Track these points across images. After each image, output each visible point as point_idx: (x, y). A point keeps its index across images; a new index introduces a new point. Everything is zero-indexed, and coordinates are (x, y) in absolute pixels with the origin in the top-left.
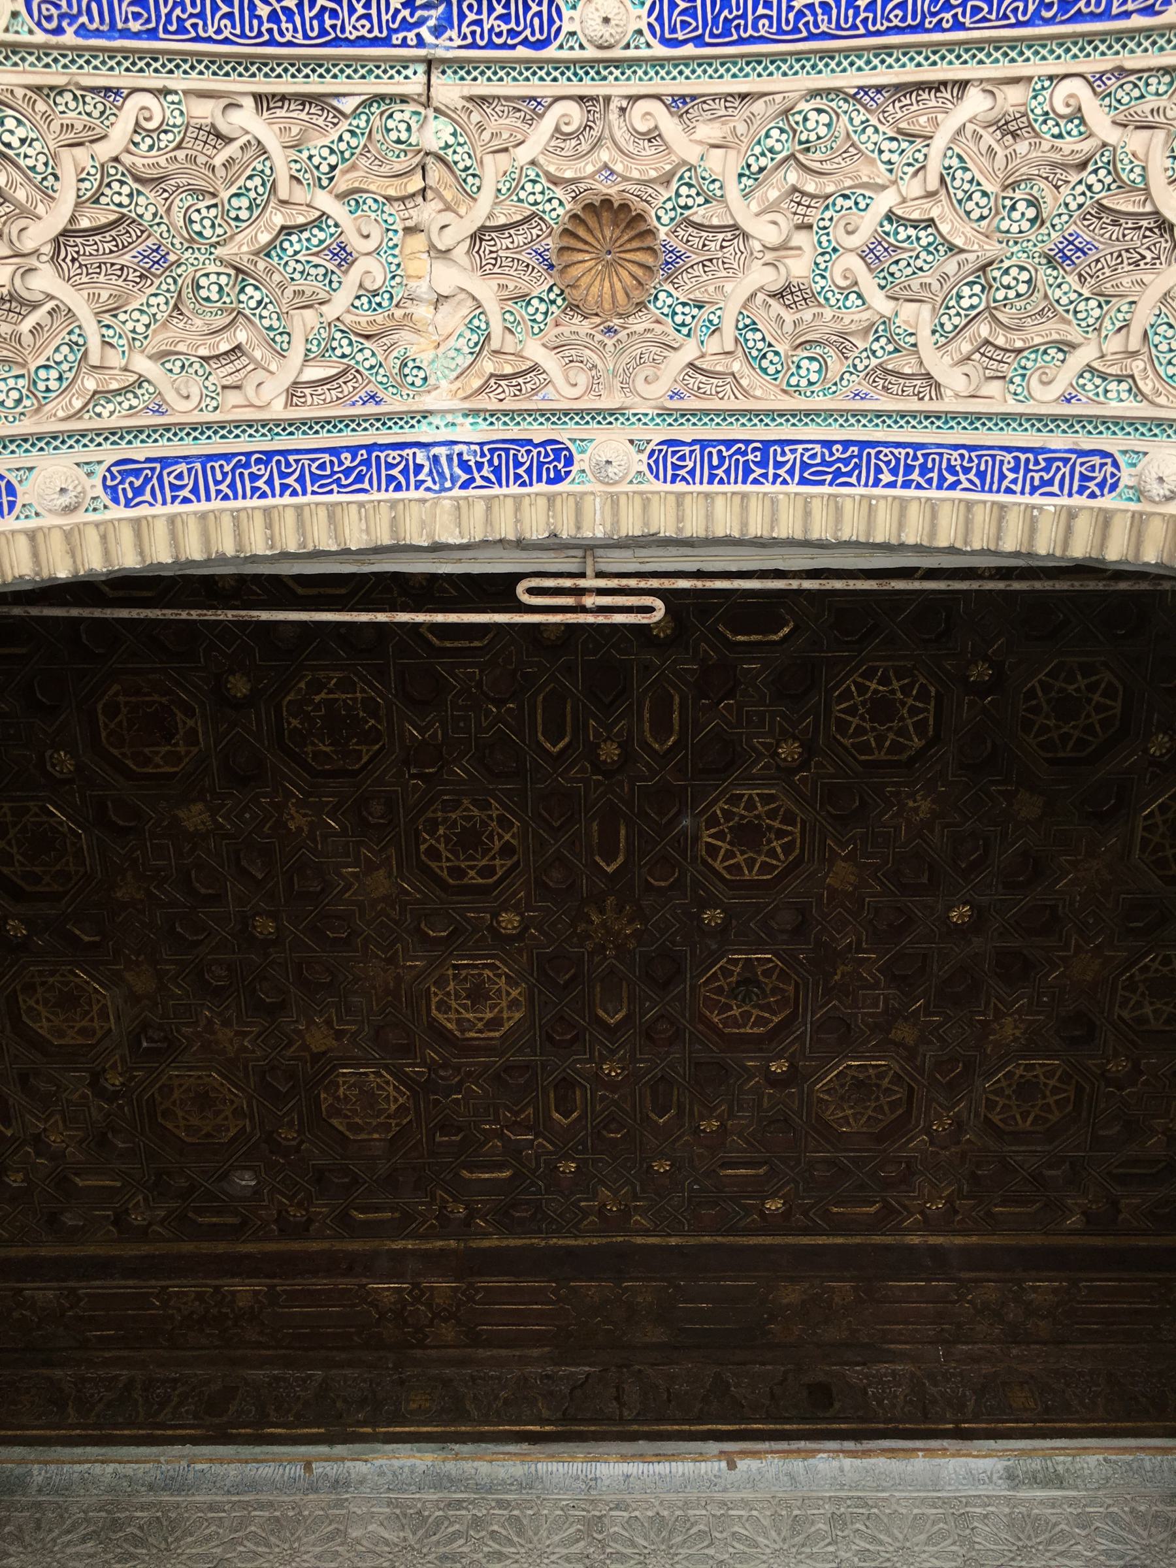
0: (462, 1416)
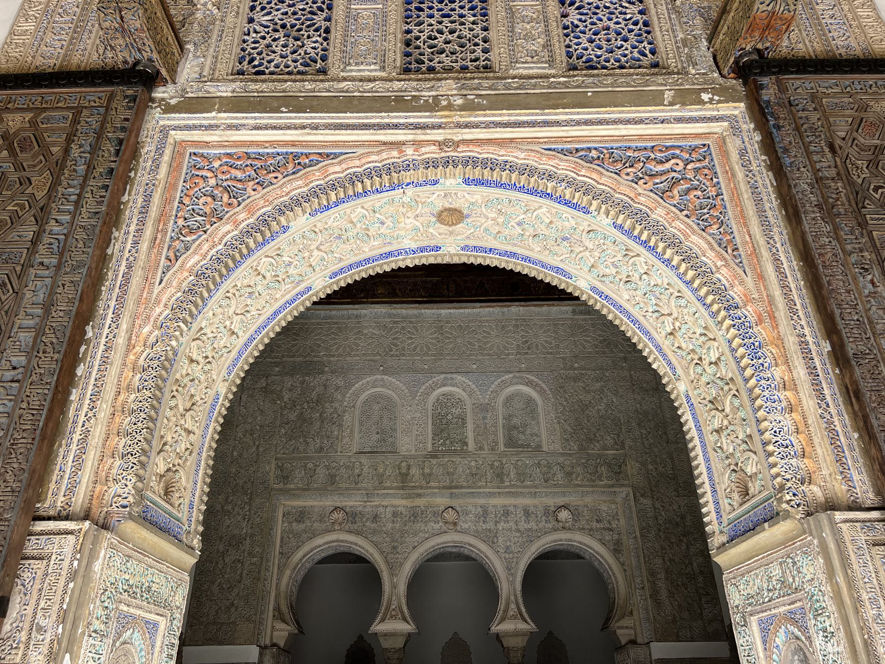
0: (396, 296)
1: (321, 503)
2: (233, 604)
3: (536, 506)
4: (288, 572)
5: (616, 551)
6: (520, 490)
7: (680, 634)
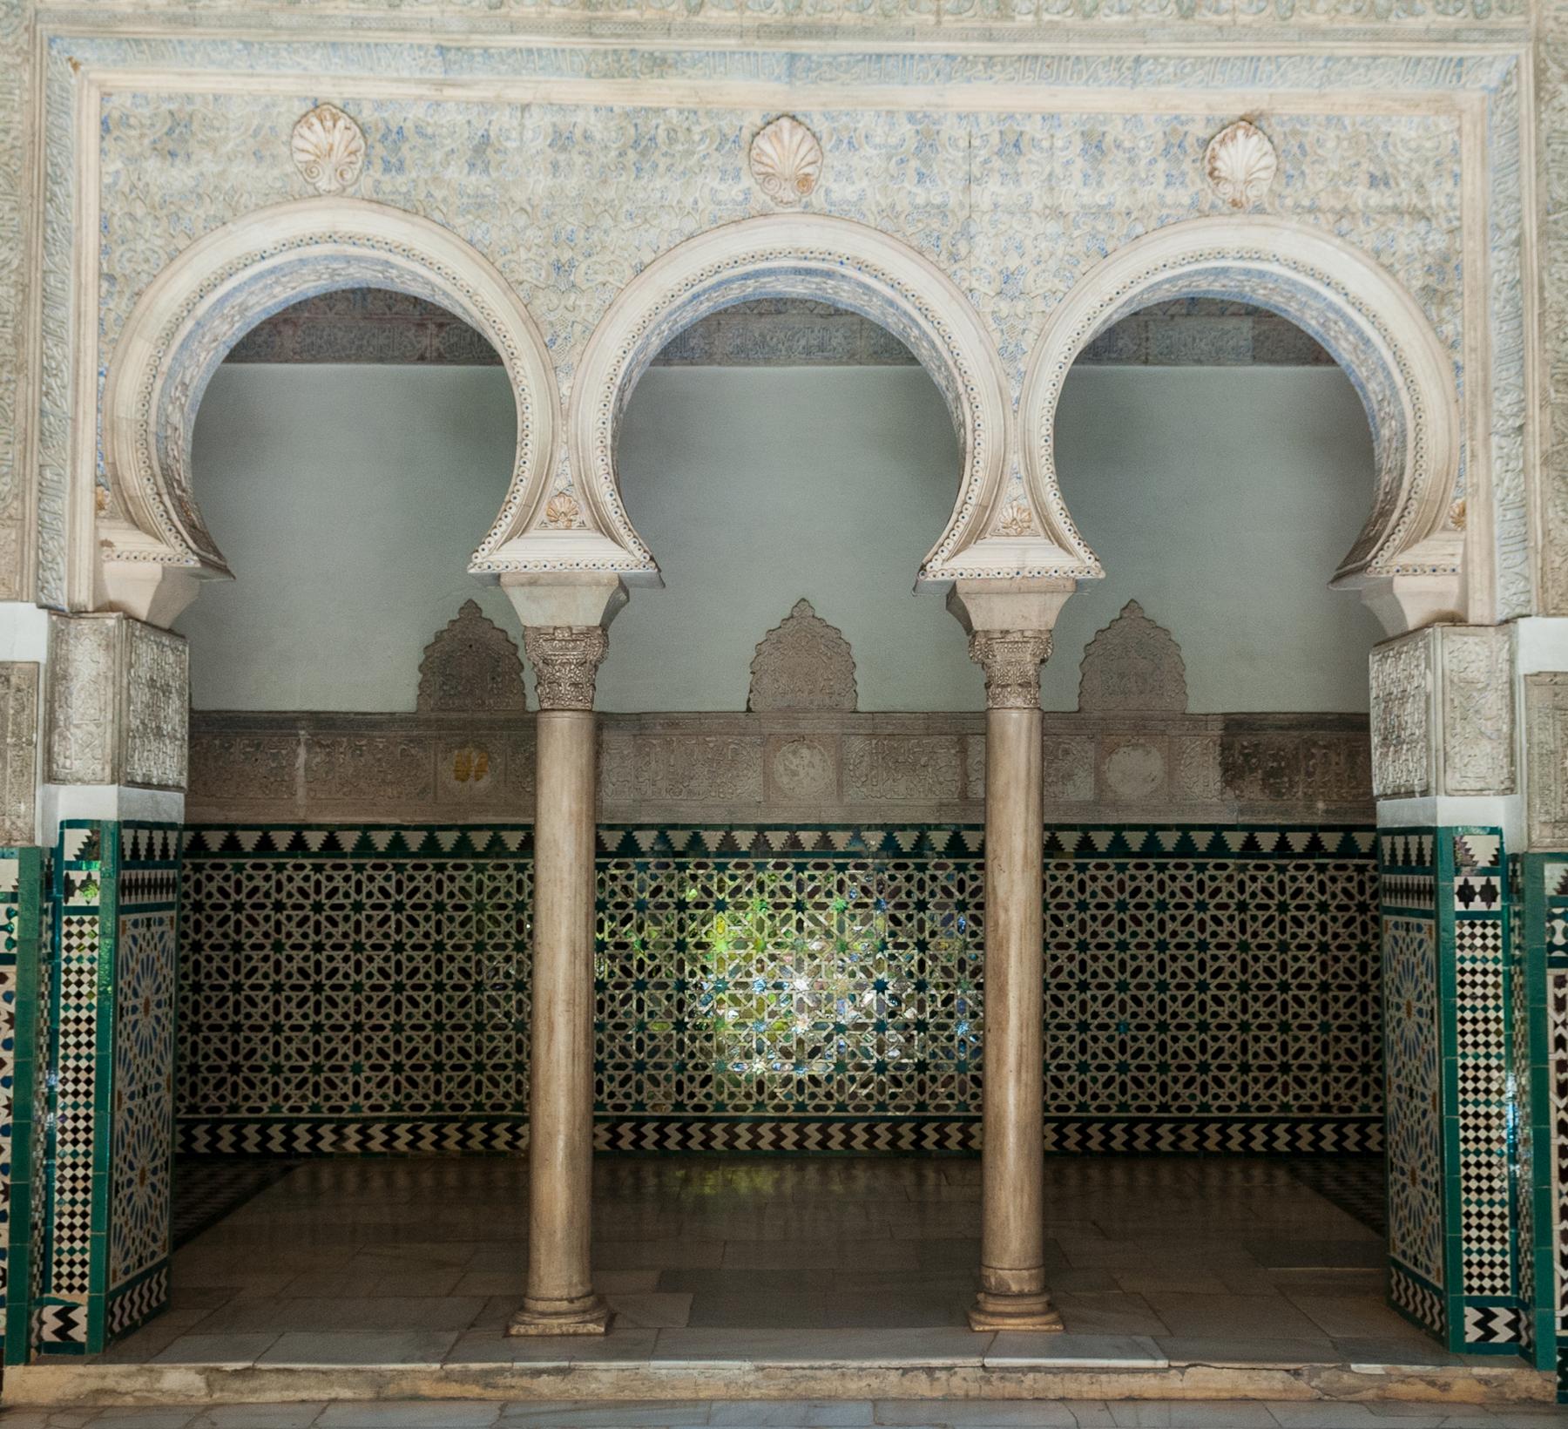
1: (255, 85)
3: (1132, 120)
4: (140, 352)
5: (1436, 292)
6: (1075, 48)
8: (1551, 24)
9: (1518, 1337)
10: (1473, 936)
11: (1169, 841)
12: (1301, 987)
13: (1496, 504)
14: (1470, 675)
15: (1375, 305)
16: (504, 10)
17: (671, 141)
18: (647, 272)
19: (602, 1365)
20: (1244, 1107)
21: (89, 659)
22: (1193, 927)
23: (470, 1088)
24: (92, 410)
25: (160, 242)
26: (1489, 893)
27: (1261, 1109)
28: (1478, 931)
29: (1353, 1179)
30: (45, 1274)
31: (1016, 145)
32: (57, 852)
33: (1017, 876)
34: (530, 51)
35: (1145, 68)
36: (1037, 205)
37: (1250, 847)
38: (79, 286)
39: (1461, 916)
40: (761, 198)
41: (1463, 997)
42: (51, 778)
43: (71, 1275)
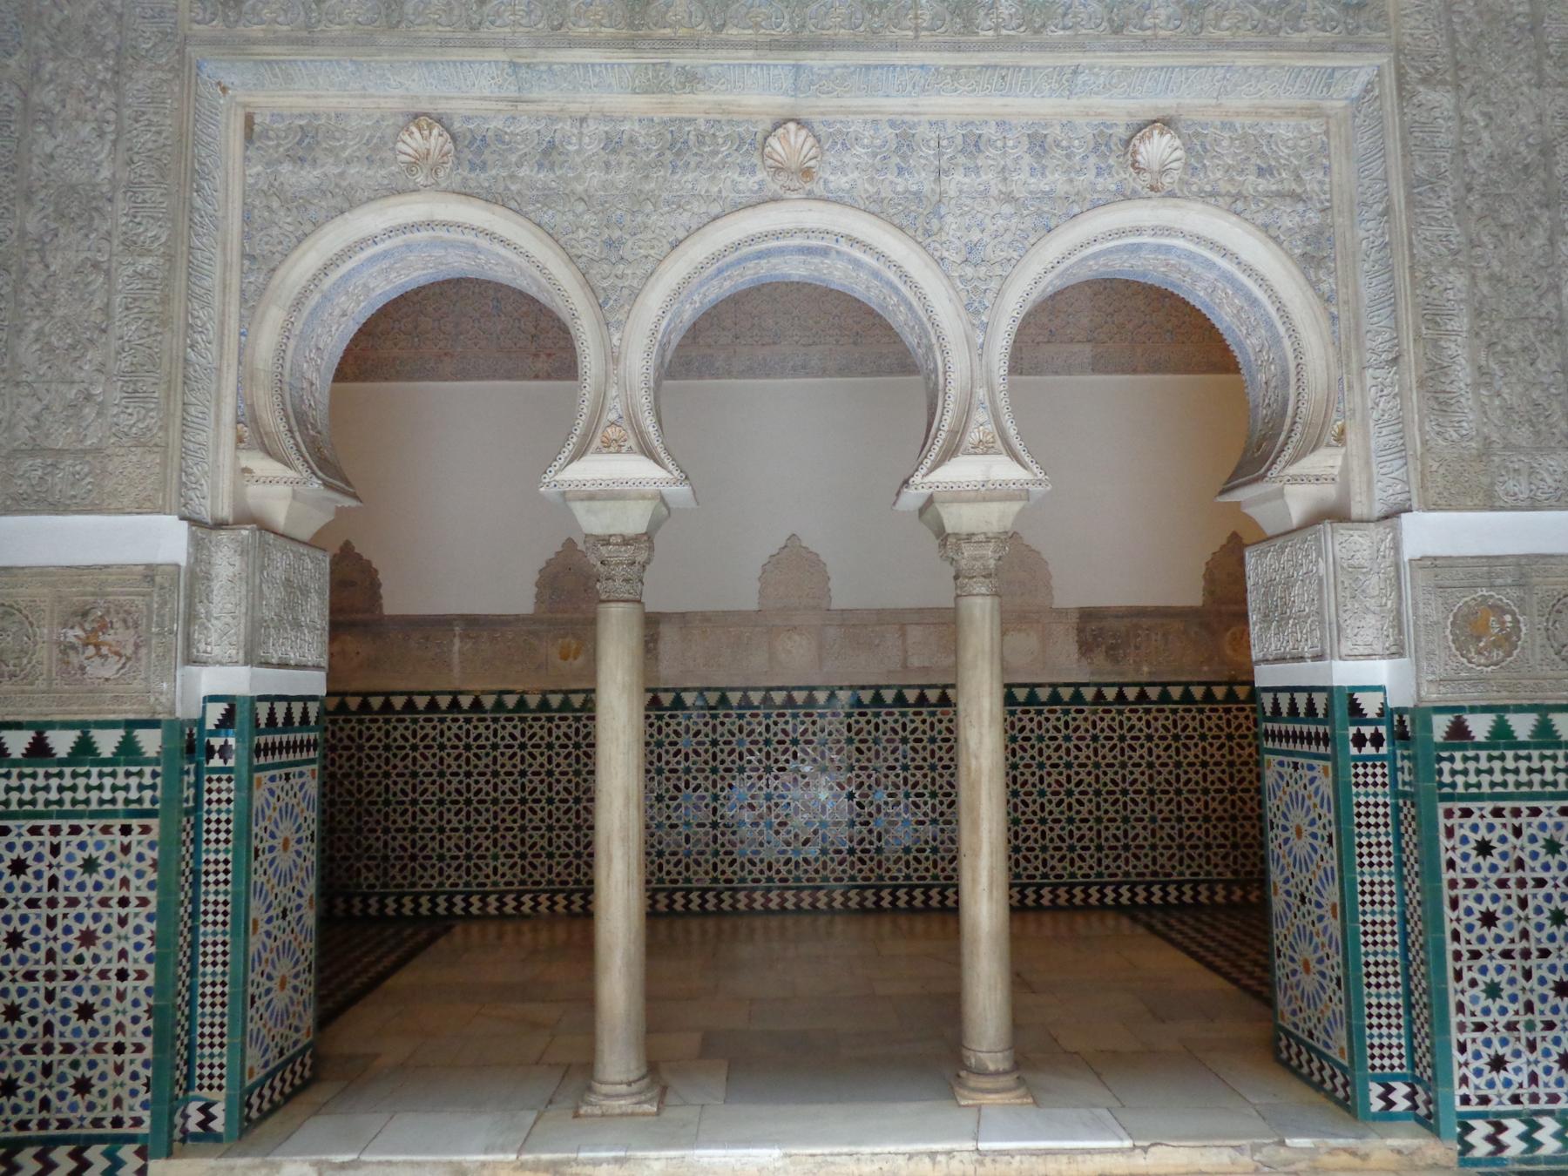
1: (368, 103)
2: (88, 397)
3: (1068, 125)
5: (1313, 257)
7: (1499, 489)
8: (1408, 39)
9: (1415, 1107)
10: (1366, 775)
11: (1043, 694)
12: (1136, 792)
13: (1372, 423)
14: (1355, 562)
15: (1262, 269)
16: (563, 30)
17: (701, 143)
18: (682, 247)
19: (653, 1154)
20: (1099, 875)
21: (226, 561)
22: (1062, 752)
23: (572, 870)
24: (234, 362)
25: (291, 228)
26: (1377, 740)
27: (1111, 875)
28: (1370, 770)
29: (1173, 922)
30: (188, 1077)
31: (976, 145)
32: (201, 722)
33: (985, 731)
34: (585, 66)
35: (1081, 79)
36: (994, 192)
37: (1099, 698)
38: (225, 265)
39: (1355, 758)
40: (774, 187)
41: (1359, 825)
42: (191, 660)
43: (211, 1076)
